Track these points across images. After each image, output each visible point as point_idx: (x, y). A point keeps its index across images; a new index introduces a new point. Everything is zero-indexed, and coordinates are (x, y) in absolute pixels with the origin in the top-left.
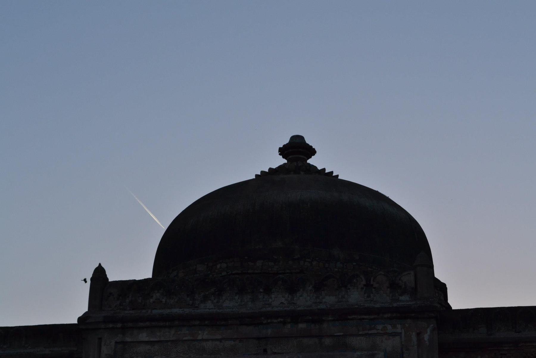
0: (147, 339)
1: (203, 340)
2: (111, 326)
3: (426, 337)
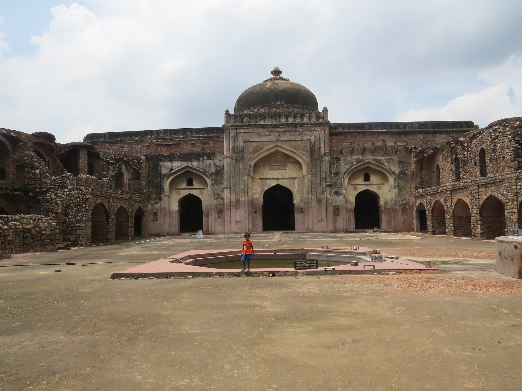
3: (327, 131)
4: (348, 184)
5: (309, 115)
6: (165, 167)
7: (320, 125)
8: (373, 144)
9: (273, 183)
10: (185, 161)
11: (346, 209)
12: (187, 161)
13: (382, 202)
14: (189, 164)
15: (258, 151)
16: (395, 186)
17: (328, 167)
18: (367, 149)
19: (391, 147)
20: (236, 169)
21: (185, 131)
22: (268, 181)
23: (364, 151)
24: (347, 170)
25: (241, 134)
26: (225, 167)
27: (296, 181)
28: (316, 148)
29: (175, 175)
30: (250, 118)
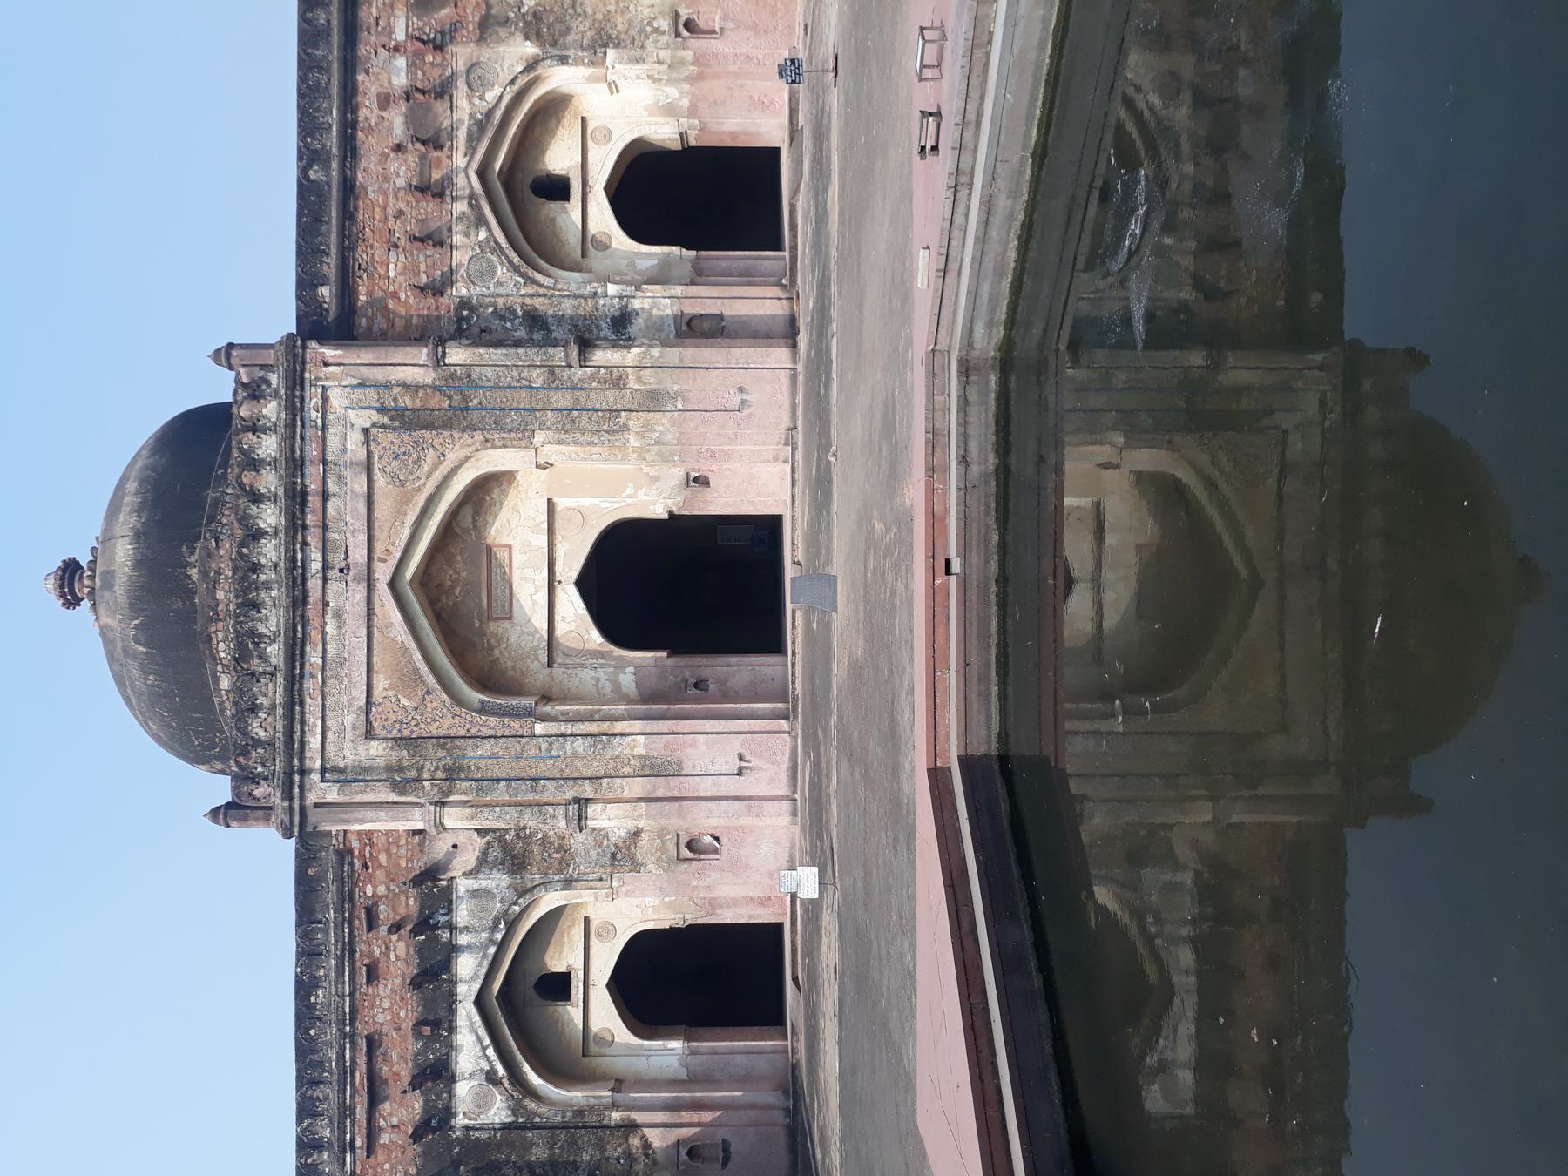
0: (319, 737)
1: (324, 658)
2: (296, 790)
3: (329, 353)
4: (580, 271)
5: (246, 429)
6: (479, 1103)
7: (296, 381)
8: (399, 148)
9: (572, 606)
10: (452, 1012)
11: (693, 283)
12: (451, 1001)
13: (664, 133)
14: (466, 991)
15: (416, 670)
16: (592, 63)
17: (496, 354)
18: (421, 174)
19: (412, 67)
20: (499, 775)
21: (305, 1014)
22: (560, 629)
23: (432, 190)
24: (516, 269)
25: (330, 748)
26: (488, 825)
27: (561, 503)
28: (407, 401)
29: (520, 1057)
30: (254, 709)
